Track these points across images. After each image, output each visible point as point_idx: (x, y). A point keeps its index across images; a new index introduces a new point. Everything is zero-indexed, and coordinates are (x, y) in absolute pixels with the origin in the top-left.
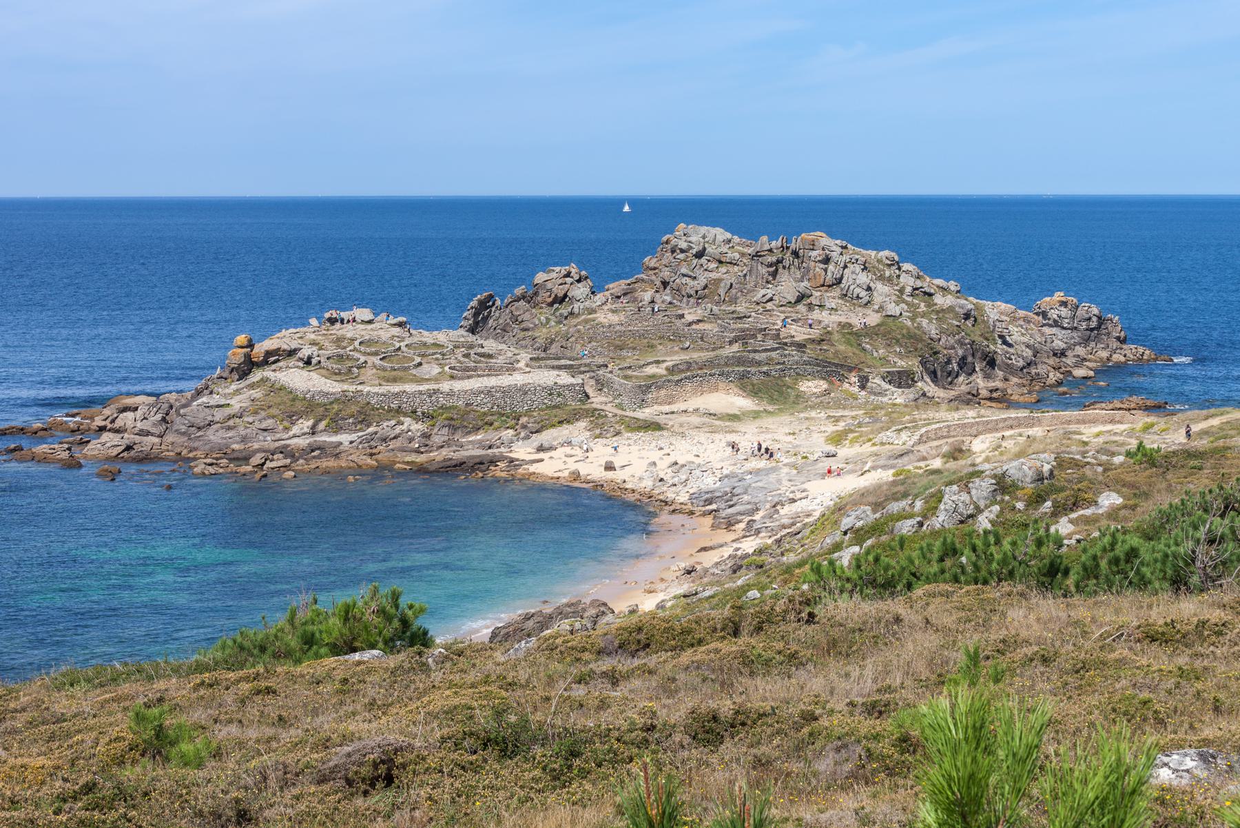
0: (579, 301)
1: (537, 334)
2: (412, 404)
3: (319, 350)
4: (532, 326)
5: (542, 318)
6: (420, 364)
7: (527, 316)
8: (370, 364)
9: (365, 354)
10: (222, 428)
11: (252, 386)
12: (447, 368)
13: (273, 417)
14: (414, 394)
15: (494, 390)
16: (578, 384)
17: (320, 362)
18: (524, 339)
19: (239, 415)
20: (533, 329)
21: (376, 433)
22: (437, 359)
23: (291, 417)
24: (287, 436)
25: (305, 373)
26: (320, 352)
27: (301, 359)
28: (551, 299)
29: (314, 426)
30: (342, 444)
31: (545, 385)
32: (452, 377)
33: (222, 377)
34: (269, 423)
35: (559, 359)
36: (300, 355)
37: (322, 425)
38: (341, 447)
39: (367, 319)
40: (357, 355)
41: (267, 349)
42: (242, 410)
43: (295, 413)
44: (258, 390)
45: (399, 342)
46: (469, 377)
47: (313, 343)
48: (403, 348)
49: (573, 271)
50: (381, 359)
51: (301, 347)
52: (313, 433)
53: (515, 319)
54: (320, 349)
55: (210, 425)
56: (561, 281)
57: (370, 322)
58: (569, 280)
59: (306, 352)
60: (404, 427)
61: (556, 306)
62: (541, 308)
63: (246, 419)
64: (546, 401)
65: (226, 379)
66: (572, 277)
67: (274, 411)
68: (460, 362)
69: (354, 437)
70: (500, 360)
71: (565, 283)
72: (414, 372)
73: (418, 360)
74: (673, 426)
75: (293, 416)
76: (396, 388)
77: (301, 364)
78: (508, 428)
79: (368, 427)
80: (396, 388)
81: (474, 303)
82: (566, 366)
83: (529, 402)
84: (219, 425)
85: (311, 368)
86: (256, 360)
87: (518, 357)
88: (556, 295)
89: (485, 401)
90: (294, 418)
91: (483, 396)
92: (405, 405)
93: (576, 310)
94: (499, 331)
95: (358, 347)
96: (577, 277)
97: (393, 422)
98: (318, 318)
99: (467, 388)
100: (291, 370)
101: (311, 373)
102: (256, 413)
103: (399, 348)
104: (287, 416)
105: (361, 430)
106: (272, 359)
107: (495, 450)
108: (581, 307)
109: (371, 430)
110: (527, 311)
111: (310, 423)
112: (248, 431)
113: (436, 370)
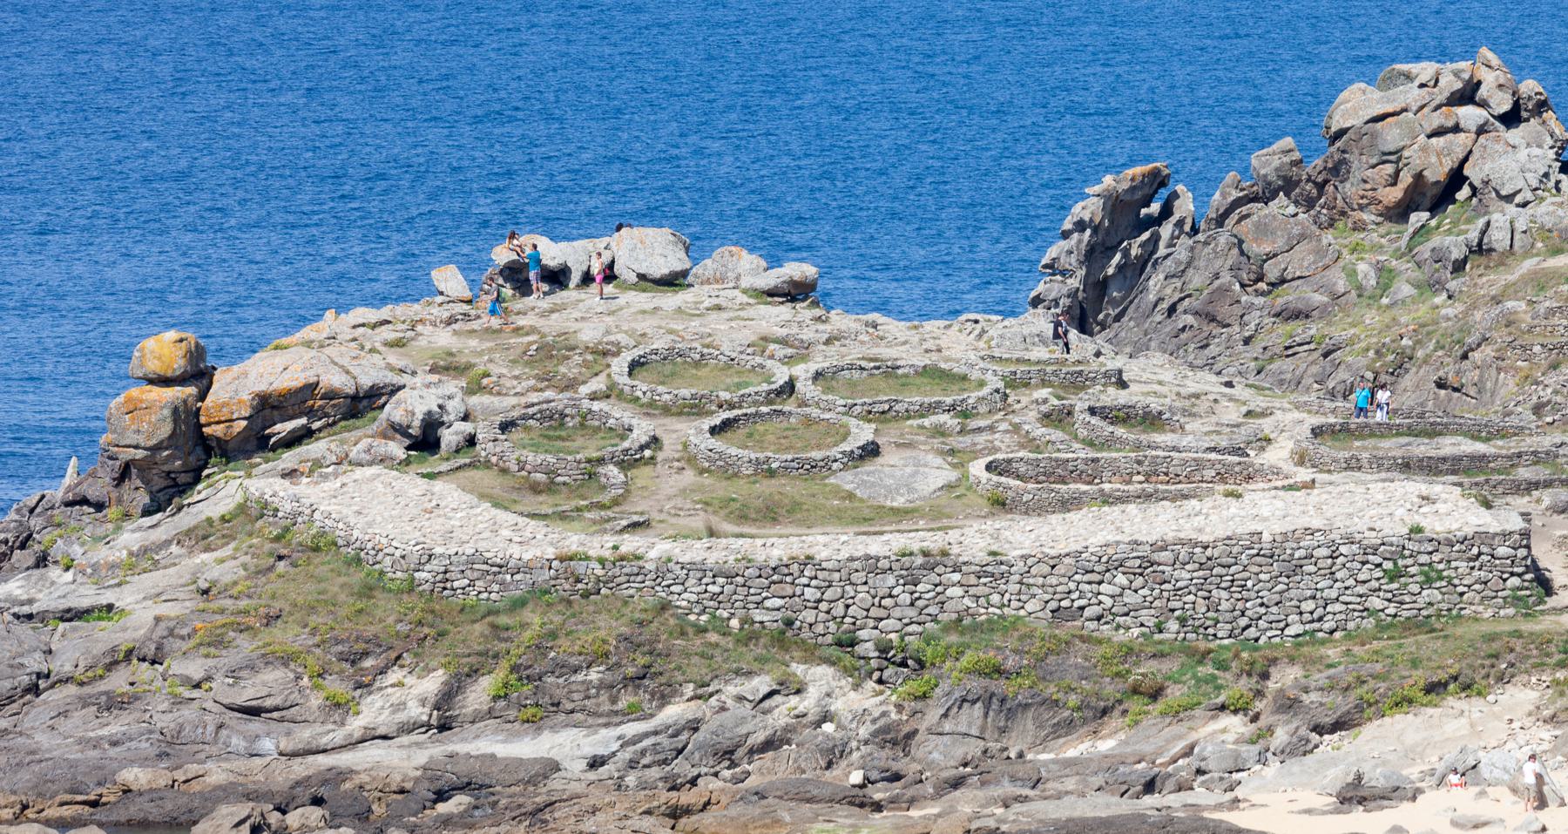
0: (1509, 198)
1: (1339, 331)
2: (839, 610)
3: (469, 392)
4: (1319, 298)
5: (1362, 267)
6: (871, 451)
7: (1299, 261)
8: (670, 448)
9: (652, 408)
10: (85, 703)
11: (202, 536)
12: (977, 469)
13: (286, 660)
15: (1165, 556)
16: (1506, 535)
17: (471, 441)
18: (1289, 351)
19: (150, 650)
20: (1324, 312)
21: (694, 726)
22: (939, 431)
23: (354, 659)
24: (338, 736)
25: (411, 485)
26: (474, 400)
27: (399, 430)
28: (1395, 194)
29: (446, 699)
30: (555, 767)
31: (1372, 539)
32: (1000, 504)
33: (84, 501)
34: (267, 684)
35: (1433, 432)
36: (394, 411)
37: (478, 694)
38: (556, 783)
39: (660, 269)
40: (618, 413)
41: (262, 387)
42: (161, 631)
43: (371, 645)
44: (227, 551)
45: (789, 360)
46: (1067, 504)
47: (447, 367)
48: (805, 388)
49: (1489, 79)
50: (714, 431)
51: (398, 380)
52: (444, 727)
53: (1256, 277)
54: (475, 388)
55: (34, 690)
56: (1437, 120)
57: (672, 281)
58: (1469, 115)
59: (413, 405)
60: (808, 703)
61: (1418, 218)
62: (1359, 227)
63: (177, 667)
64: (1375, 602)
65: (99, 507)
66: (1483, 104)
67: (287, 636)
68: (1030, 443)
69: (603, 740)
70: (1194, 437)
71: (1456, 129)
72: (846, 480)
73: (863, 433)
75: (366, 654)
76: (774, 547)
77: (397, 449)
78: (1223, 708)
79: (664, 699)
80: (774, 547)
81: (1088, 207)
82: (1457, 459)
83: (1308, 606)
84: (72, 689)
85: (434, 464)
87: (1266, 425)
88: (1419, 177)
89: (1130, 598)
90: (368, 663)
91: (1121, 579)
92: (809, 616)
93: (1498, 238)
94: (1189, 319)
95: (624, 380)
96: (1503, 104)
97: (761, 684)
98: (469, 267)
99: (1061, 548)
100: (359, 473)
101: (438, 486)
102: (218, 642)
103: (790, 387)
104: (342, 658)
105: (633, 713)
106: (284, 428)
107: (1174, 800)
108: (1521, 225)
109: (675, 712)
110: (1302, 237)
111: (432, 684)
112: (188, 713)
113: (935, 474)
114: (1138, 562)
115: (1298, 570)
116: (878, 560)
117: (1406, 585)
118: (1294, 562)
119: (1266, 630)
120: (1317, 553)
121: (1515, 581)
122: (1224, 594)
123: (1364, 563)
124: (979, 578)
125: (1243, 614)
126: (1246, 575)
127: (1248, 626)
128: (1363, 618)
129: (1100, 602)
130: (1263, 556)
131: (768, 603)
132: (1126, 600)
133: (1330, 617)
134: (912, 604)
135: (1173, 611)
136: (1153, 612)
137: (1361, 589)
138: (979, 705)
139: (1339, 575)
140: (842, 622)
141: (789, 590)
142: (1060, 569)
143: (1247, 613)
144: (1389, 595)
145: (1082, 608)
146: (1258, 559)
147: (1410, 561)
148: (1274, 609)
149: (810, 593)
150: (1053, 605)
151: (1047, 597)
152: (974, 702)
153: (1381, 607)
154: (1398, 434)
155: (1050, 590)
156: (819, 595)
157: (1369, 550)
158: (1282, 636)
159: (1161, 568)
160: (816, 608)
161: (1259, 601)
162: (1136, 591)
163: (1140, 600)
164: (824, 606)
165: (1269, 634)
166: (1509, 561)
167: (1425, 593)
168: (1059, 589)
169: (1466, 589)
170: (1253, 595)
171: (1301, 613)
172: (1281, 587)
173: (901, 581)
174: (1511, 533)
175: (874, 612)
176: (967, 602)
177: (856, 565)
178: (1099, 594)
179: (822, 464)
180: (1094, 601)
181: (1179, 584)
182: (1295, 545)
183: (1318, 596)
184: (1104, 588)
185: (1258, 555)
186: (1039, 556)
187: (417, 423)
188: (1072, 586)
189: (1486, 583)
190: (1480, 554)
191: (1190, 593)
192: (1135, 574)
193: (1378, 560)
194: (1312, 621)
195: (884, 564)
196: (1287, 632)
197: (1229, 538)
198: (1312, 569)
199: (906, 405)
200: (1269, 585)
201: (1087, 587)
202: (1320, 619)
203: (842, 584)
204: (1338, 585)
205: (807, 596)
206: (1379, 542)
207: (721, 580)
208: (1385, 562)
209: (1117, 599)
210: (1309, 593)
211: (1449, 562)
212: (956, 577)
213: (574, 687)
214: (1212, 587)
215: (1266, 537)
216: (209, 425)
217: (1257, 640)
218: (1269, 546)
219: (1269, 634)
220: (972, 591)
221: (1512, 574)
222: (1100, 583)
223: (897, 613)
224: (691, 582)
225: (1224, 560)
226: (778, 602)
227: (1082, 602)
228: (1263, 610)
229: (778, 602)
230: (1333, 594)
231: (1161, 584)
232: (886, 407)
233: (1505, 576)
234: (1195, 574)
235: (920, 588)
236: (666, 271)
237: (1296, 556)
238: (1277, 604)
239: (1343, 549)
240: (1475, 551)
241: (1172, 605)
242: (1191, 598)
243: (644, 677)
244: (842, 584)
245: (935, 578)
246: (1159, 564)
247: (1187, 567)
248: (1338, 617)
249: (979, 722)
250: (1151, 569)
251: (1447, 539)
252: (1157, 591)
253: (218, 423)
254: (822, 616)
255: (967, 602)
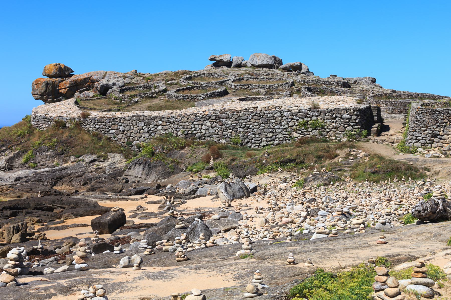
14: (131, 119)
16: (347, 110)
31: (295, 110)
37: (22, 160)
74: (437, 173)
78: (212, 168)
79: (66, 162)
86: (62, 91)
89: (211, 131)
91: (209, 124)
97: (94, 157)
114: (214, 117)
115: (269, 122)
116: (140, 117)
117: (307, 128)
118: (267, 118)
119: (254, 143)
120: (276, 115)
121: (350, 128)
122: (242, 130)
123: (292, 119)
124: (167, 123)
125: (247, 138)
126: (250, 123)
127: (249, 142)
128: (289, 140)
129: (201, 132)
130: (257, 116)
131: (110, 132)
132: (209, 131)
133: (277, 139)
134: (148, 132)
135: (224, 135)
136: (218, 136)
137: (289, 129)
138: (142, 166)
139: (283, 124)
140: (129, 139)
141: (116, 127)
142: (190, 120)
143: (249, 137)
144: (300, 132)
145: (195, 134)
146: (255, 117)
147: (309, 119)
148: (257, 136)
149: (122, 129)
150: (186, 132)
151: (184, 129)
152: (140, 164)
153: (296, 136)
154: (411, 98)
155: (186, 127)
156: (124, 128)
157: (294, 114)
158: (259, 146)
159: (222, 120)
160: (123, 133)
161: (253, 132)
162: (213, 128)
163: (214, 131)
164: (125, 133)
165: (254, 145)
166: (347, 120)
167: (313, 131)
168: (189, 127)
169: (329, 130)
170: (251, 130)
171: (267, 138)
172: (262, 127)
173: (146, 124)
174: (349, 109)
175: (138, 135)
176: (163, 132)
177: (134, 118)
178: (201, 129)
179: (195, 97)
180: (199, 131)
181: (228, 126)
182: (268, 112)
183: (274, 131)
184: (204, 127)
185: (255, 115)
186: (184, 115)
187: (99, 87)
188: (193, 126)
189: (337, 128)
190: (336, 117)
191: (230, 129)
192: (213, 122)
193: (297, 118)
194: (271, 141)
195: (142, 118)
196: (261, 145)
197: (246, 109)
198: (273, 121)
199: (254, 86)
200: (258, 127)
201: (197, 126)
202: (274, 140)
203: (130, 125)
204: (282, 127)
205: (121, 129)
206: (298, 111)
207: (99, 124)
208: (300, 119)
209: (207, 131)
210: (270, 130)
211: (324, 120)
212: (160, 122)
213: (43, 157)
214: (237, 127)
215: (259, 109)
216: (61, 89)
217: (250, 147)
218: (259, 112)
219: (254, 145)
220: (165, 127)
221: (349, 125)
222: (202, 125)
223: (143, 135)
224: (92, 124)
225: (243, 117)
226: (113, 131)
227: (195, 132)
228: (254, 136)
229: (113, 131)
230: (279, 131)
231: (221, 126)
232: (247, 86)
233: (346, 126)
234: (233, 122)
235: (151, 127)
236: (260, 64)
237: (268, 116)
238: (259, 134)
239: (285, 114)
240: (334, 115)
241: (225, 133)
242: (231, 131)
243: (62, 154)
244: (130, 125)
245: (155, 123)
246: (222, 118)
247: (231, 120)
248: (280, 139)
249: (141, 172)
250: (219, 120)
251: (324, 111)
252: (220, 128)
253: (63, 89)
254: (124, 136)
255: (163, 132)
